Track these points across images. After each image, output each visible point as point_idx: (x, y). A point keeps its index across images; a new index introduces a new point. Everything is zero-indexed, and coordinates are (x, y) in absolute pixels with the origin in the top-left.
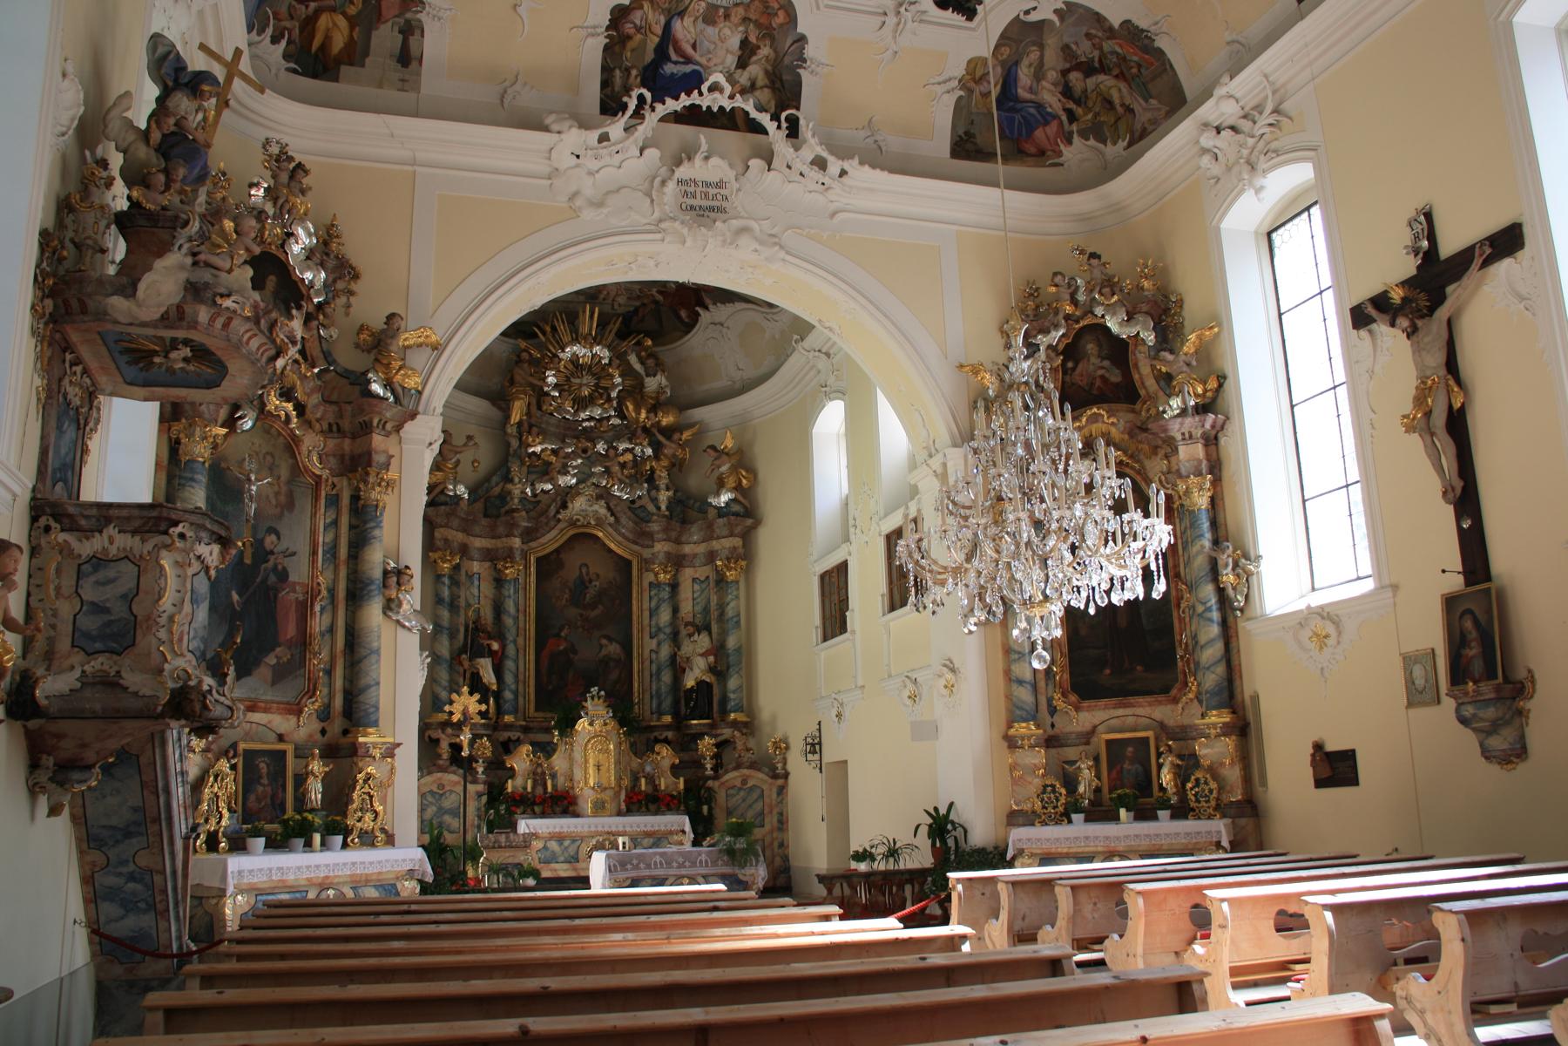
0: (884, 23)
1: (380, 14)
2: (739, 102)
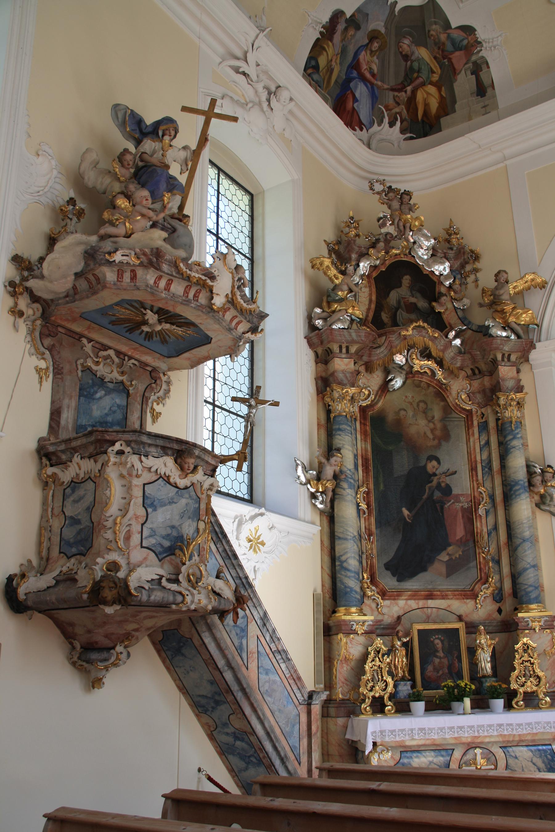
1: (454, 69)
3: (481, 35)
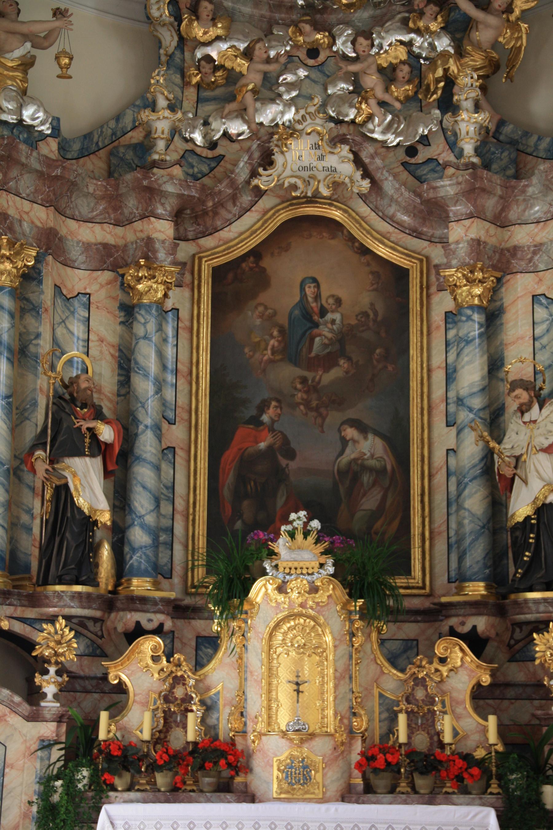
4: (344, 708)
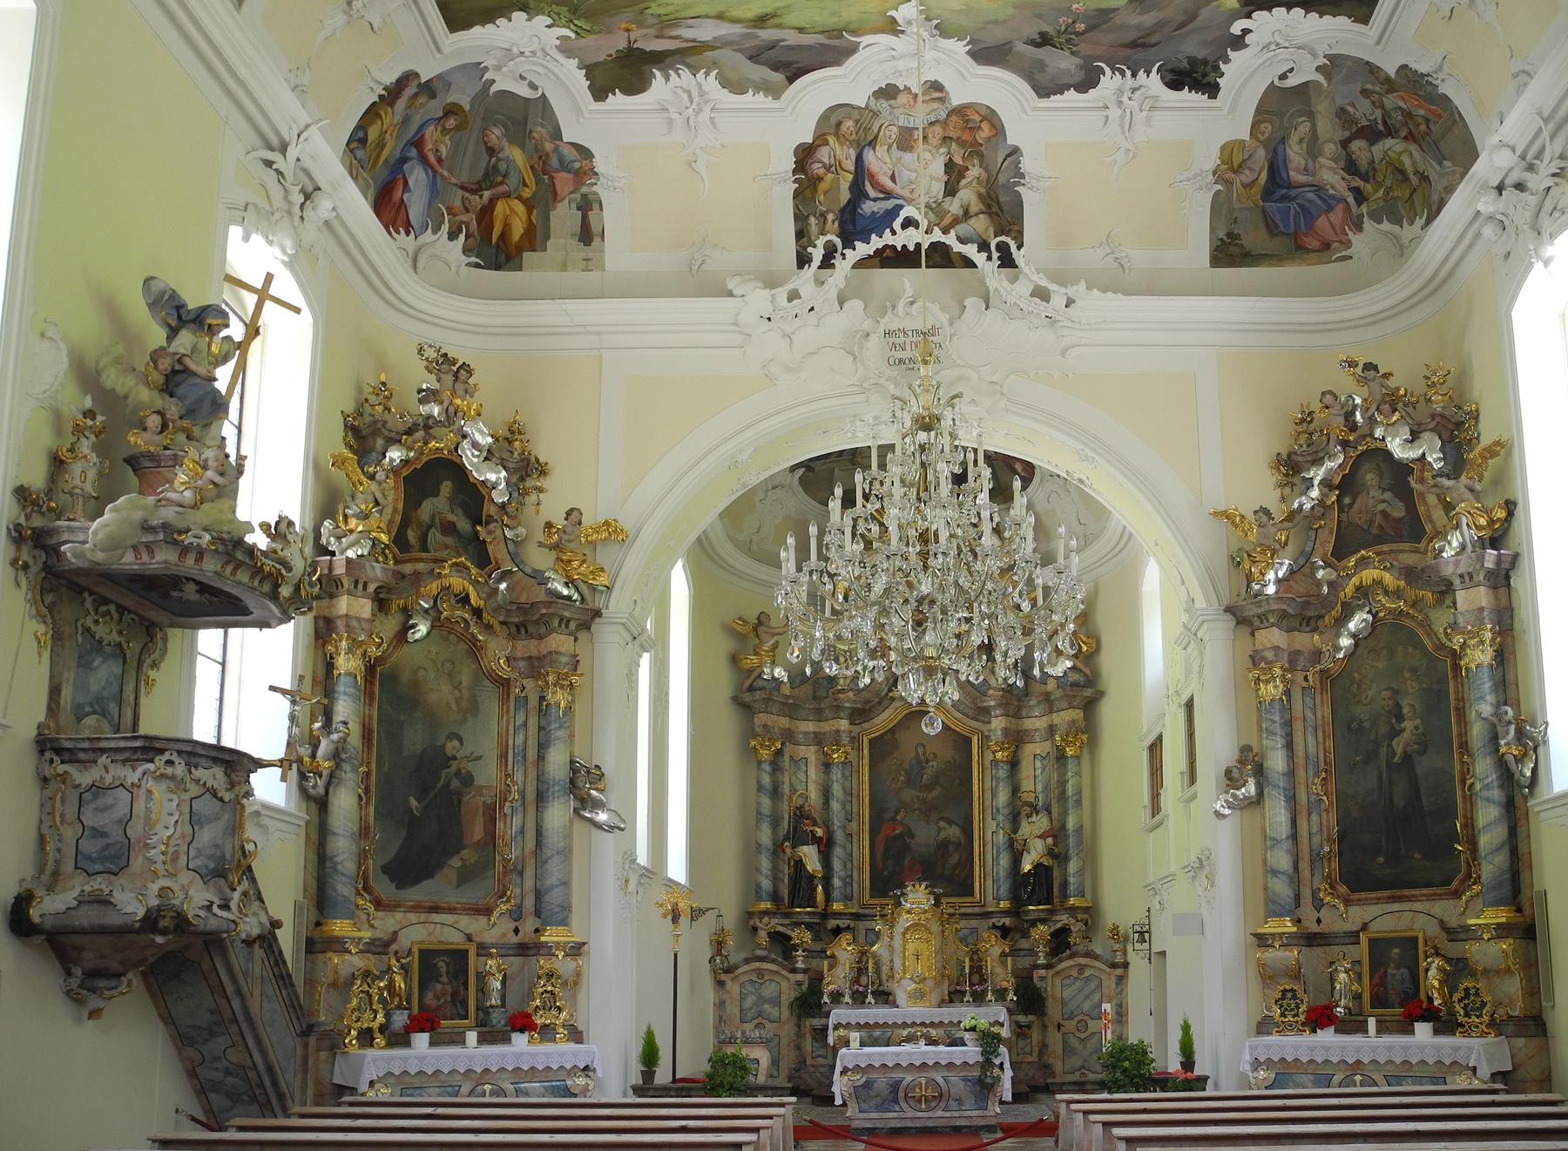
0: (1107, 117)
1: (555, 193)
2: (937, 236)
3: (600, 164)
4: (939, 966)
